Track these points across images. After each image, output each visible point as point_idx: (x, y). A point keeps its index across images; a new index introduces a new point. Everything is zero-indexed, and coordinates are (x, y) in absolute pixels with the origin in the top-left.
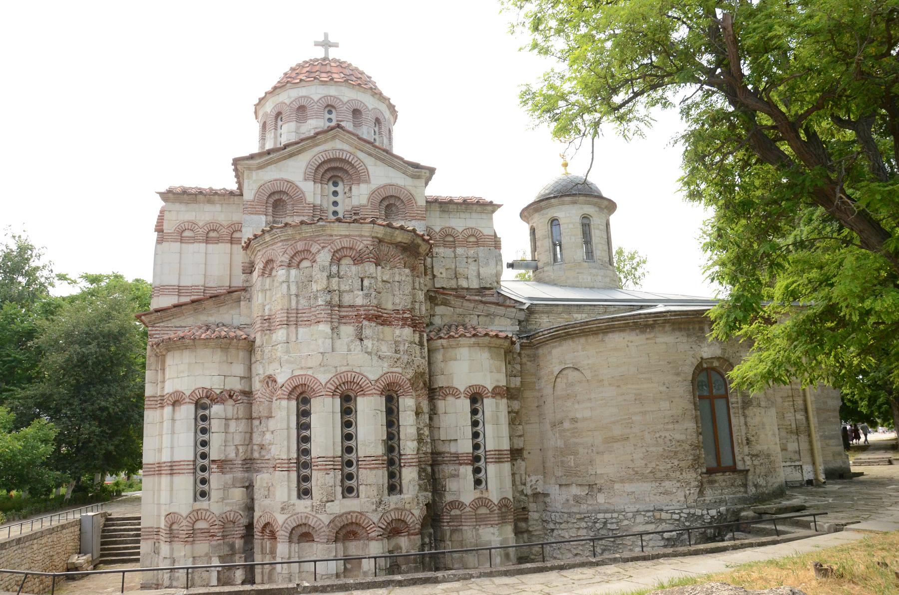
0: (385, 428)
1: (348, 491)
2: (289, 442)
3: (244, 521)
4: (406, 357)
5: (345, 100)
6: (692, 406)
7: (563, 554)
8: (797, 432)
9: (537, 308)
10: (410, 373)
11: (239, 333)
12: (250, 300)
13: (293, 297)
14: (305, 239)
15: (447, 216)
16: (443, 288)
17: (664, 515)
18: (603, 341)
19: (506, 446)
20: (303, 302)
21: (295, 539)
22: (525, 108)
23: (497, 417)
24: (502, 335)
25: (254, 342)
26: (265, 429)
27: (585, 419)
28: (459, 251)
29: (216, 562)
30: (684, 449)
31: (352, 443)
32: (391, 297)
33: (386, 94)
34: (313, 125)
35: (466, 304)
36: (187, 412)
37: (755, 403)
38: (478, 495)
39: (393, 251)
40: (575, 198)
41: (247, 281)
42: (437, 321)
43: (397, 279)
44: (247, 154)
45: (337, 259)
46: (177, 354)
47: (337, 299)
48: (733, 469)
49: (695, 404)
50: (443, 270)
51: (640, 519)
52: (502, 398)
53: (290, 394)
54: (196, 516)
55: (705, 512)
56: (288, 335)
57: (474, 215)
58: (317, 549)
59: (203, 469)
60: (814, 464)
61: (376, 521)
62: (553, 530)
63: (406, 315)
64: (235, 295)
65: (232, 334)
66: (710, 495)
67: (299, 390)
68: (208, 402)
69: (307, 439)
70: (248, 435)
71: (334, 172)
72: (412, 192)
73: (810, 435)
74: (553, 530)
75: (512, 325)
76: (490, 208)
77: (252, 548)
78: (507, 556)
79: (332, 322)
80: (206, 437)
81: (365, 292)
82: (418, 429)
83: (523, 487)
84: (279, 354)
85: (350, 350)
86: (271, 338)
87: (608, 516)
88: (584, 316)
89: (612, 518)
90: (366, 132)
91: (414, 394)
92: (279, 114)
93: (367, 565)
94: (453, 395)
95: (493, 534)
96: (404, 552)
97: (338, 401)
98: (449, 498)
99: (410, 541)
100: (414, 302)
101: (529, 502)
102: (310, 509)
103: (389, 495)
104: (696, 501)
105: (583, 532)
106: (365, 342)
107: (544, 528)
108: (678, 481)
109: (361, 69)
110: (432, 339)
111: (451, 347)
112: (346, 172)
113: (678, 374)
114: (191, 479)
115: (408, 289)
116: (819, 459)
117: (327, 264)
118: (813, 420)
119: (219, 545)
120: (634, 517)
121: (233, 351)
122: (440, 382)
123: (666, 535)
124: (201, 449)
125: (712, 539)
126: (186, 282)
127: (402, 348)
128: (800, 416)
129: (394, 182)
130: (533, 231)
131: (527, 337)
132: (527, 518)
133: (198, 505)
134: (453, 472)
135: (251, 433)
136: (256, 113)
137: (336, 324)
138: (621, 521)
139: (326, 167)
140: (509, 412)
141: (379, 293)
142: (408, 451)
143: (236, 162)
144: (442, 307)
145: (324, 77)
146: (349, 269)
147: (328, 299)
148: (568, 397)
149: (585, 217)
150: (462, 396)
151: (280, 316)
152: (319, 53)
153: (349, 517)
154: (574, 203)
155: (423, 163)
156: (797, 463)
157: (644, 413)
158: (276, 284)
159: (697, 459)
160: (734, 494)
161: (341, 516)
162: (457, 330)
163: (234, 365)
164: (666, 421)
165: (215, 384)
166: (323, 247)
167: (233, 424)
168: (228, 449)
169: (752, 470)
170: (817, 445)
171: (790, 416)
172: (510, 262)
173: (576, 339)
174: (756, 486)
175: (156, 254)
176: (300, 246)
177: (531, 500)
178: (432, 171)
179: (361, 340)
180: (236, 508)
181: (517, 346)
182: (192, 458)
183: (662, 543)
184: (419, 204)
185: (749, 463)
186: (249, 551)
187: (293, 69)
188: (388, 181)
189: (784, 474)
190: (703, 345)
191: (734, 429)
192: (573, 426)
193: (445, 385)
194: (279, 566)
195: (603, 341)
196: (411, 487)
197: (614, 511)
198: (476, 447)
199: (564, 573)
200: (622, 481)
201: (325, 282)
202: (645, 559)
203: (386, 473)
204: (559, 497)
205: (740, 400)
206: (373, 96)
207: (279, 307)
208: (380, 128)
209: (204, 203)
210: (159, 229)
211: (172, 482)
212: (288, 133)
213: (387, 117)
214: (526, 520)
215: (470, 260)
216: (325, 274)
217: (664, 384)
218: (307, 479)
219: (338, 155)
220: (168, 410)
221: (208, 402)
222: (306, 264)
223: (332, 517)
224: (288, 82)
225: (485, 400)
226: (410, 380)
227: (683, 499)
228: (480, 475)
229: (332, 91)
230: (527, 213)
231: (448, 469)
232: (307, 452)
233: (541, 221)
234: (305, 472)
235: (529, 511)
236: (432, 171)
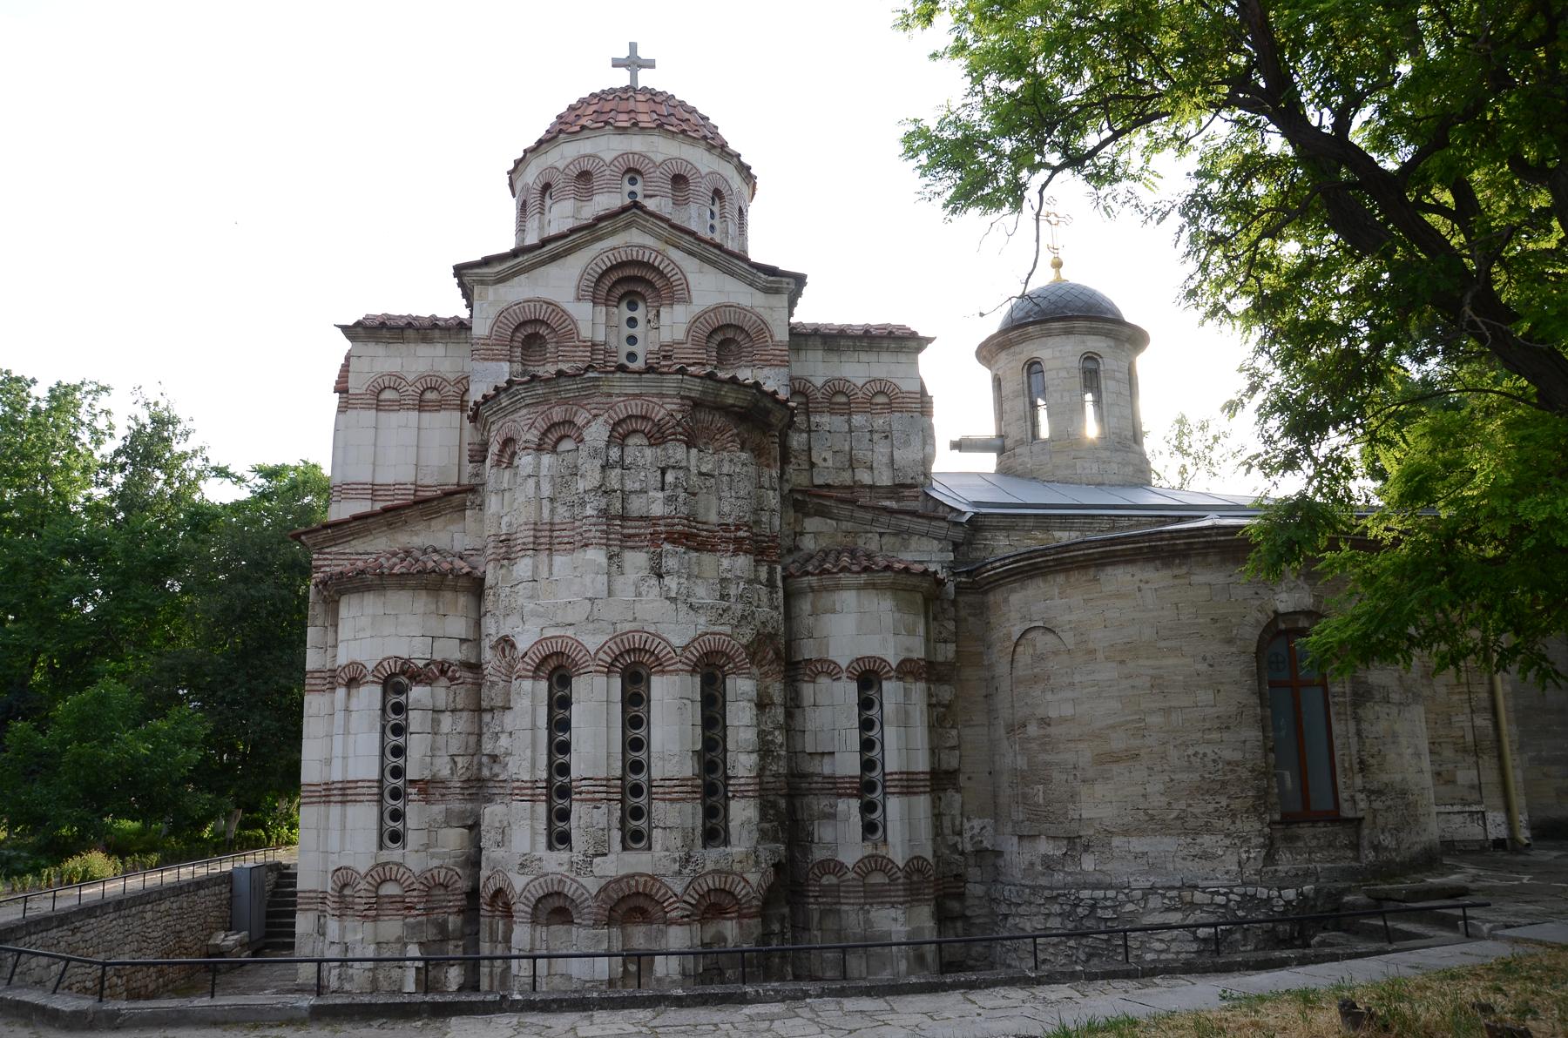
0: (699, 730)
1: (634, 839)
2: (534, 750)
3: (463, 884)
4: (740, 606)
5: (659, 159)
6: (1255, 700)
7: (1021, 959)
8: (1477, 750)
9: (987, 521)
10: (747, 635)
11: (458, 563)
12: (481, 507)
13: (546, 504)
14: (565, 401)
15: (836, 359)
16: (828, 486)
17: (1199, 897)
18: (1095, 580)
19: (922, 764)
20: (562, 510)
21: (543, 919)
22: (913, 163)
23: (907, 713)
24: (918, 568)
25: (481, 581)
26: (498, 729)
27: (1063, 720)
28: (858, 420)
29: (413, 951)
30: (1239, 779)
31: (641, 755)
32: (714, 500)
33: (733, 146)
34: (605, 202)
35: (859, 514)
36: (369, 697)
37: (1378, 697)
38: (869, 850)
39: (720, 421)
40: (1070, 324)
41: (477, 475)
42: (808, 544)
43: (725, 470)
44: (479, 258)
45: (620, 434)
47: (618, 505)
48: (1334, 818)
49: (1261, 696)
50: (828, 455)
51: (1155, 902)
52: (917, 678)
53: (538, 668)
54: (382, 873)
55: (1275, 893)
56: (536, 568)
57: (885, 357)
58: (580, 936)
59: (396, 794)
60: (1508, 810)
61: (679, 890)
62: (1006, 916)
63: (741, 534)
64: (454, 500)
65: (446, 566)
66: (1286, 863)
67: (553, 663)
68: (404, 680)
69: (565, 748)
70: (473, 739)
71: (630, 284)
72: (766, 317)
73: (1501, 757)
74: (1006, 916)
75: (941, 550)
76: (913, 344)
77: (477, 933)
78: (920, 960)
79: (608, 546)
80: (400, 740)
81: (668, 493)
82: (761, 734)
83: (957, 838)
84: (521, 601)
85: (640, 594)
86: (510, 571)
87: (1099, 894)
88: (1074, 534)
89: (1105, 899)
90: (695, 217)
91: (755, 670)
92: (547, 187)
93: (665, 968)
94: (829, 674)
95: (896, 920)
96: (730, 945)
97: (617, 682)
98: (819, 854)
99: (741, 927)
100: (758, 510)
101: (967, 866)
102: (566, 867)
103: (705, 847)
104: (1258, 872)
105: (1055, 923)
106: (667, 580)
107: (993, 913)
108: (1227, 836)
109: (690, 103)
110: (791, 575)
111: (826, 589)
112: (650, 284)
113: (1230, 641)
114: (373, 811)
115: (744, 488)
116: (1519, 801)
117: (602, 444)
118: (1508, 730)
119: (420, 924)
120: (1145, 897)
121: (448, 595)
122: (808, 650)
123: (1202, 932)
124: (391, 761)
125: (1287, 943)
126: (386, 477)
127: (733, 591)
128: (1483, 721)
129: (733, 300)
130: (998, 382)
131: (969, 573)
132: (963, 894)
133: (385, 856)
134: (827, 810)
135: (480, 735)
136: (511, 185)
137: (616, 549)
138: (1122, 904)
139: (614, 277)
140: (929, 705)
141: (694, 494)
142: (741, 772)
143: (459, 271)
144: (817, 520)
145: (623, 120)
146: (641, 453)
147: (603, 506)
148: (1035, 679)
149: (1090, 357)
150: (844, 676)
151: (525, 536)
152: (621, 78)
153: (633, 883)
154: (1068, 332)
155: (783, 267)
156: (1474, 808)
157: (1167, 711)
158: (519, 480)
159: (1262, 795)
160: (1333, 861)
161: (618, 881)
162: (838, 559)
163: (449, 619)
164: (1207, 725)
165: (417, 651)
166: (596, 416)
167: (446, 722)
168: (437, 761)
169: (1369, 818)
170: (1515, 776)
171: (1462, 720)
172: (957, 439)
173: (1049, 578)
174: (1376, 848)
175: (336, 430)
176: (558, 414)
177: (972, 861)
178: (800, 280)
179: (660, 576)
180: (449, 862)
181: (950, 587)
182: (376, 776)
183: (1195, 947)
184: (777, 338)
185: (1362, 805)
186: (471, 936)
187: (571, 108)
188: (723, 300)
189: (1438, 824)
190: (1278, 589)
191: (1337, 743)
192: (1042, 732)
193: (814, 656)
194: (514, 963)
195: (1095, 580)
196: (745, 833)
197: (1110, 887)
198: (867, 765)
199: (976, 996)
200: (1126, 833)
201: (597, 475)
202: (1128, 975)
203: (700, 809)
204: (1019, 857)
205: (1347, 690)
206: (709, 150)
207: (522, 520)
208: (722, 207)
209: (416, 341)
210: (341, 388)
211: (344, 816)
212: (561, 216)
213: (735, 187)
214: (961, 896)
215: (876, 437)
216: (598, 463)
217: (1204, 659)
218: (565, 815)
219: (635, 255)
220: (341, 692)
221: (404, 680)
222: (567, 445)
223: (603, 882)
224: (561, 131)
225: (885, 684)
226: (746, 647)
227: (1235, 868)
228: (874, 816)
229: (636, 144)
230: (989, 351)
231: (822, 804)
232: (564, 769)
233: (1012, 363)
234: (560, 803)
235: (966, 882)
236: (800, 280)
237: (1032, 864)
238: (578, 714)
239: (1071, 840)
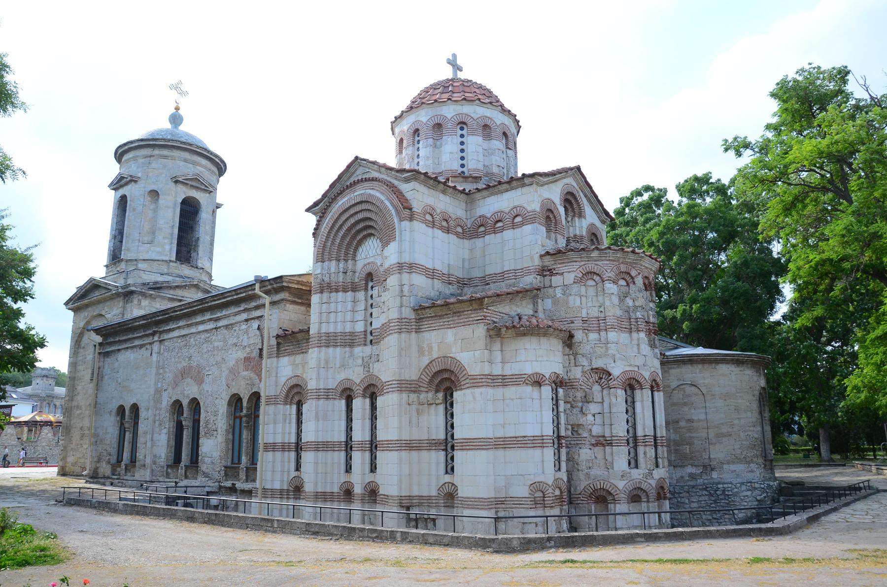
17: (757, 485)
25: (571, 336)
27: (699, 421)
36: (547, 391)
46: (534, 339)
51: (744, 488)
87: (725, 486)
148: (685, 404)
157: (739, 419)
176: (623, 268)
183: (756, 503)
200: (728, 463)
237: (682, 477)
238: (638, 405)
239: (705, 467)
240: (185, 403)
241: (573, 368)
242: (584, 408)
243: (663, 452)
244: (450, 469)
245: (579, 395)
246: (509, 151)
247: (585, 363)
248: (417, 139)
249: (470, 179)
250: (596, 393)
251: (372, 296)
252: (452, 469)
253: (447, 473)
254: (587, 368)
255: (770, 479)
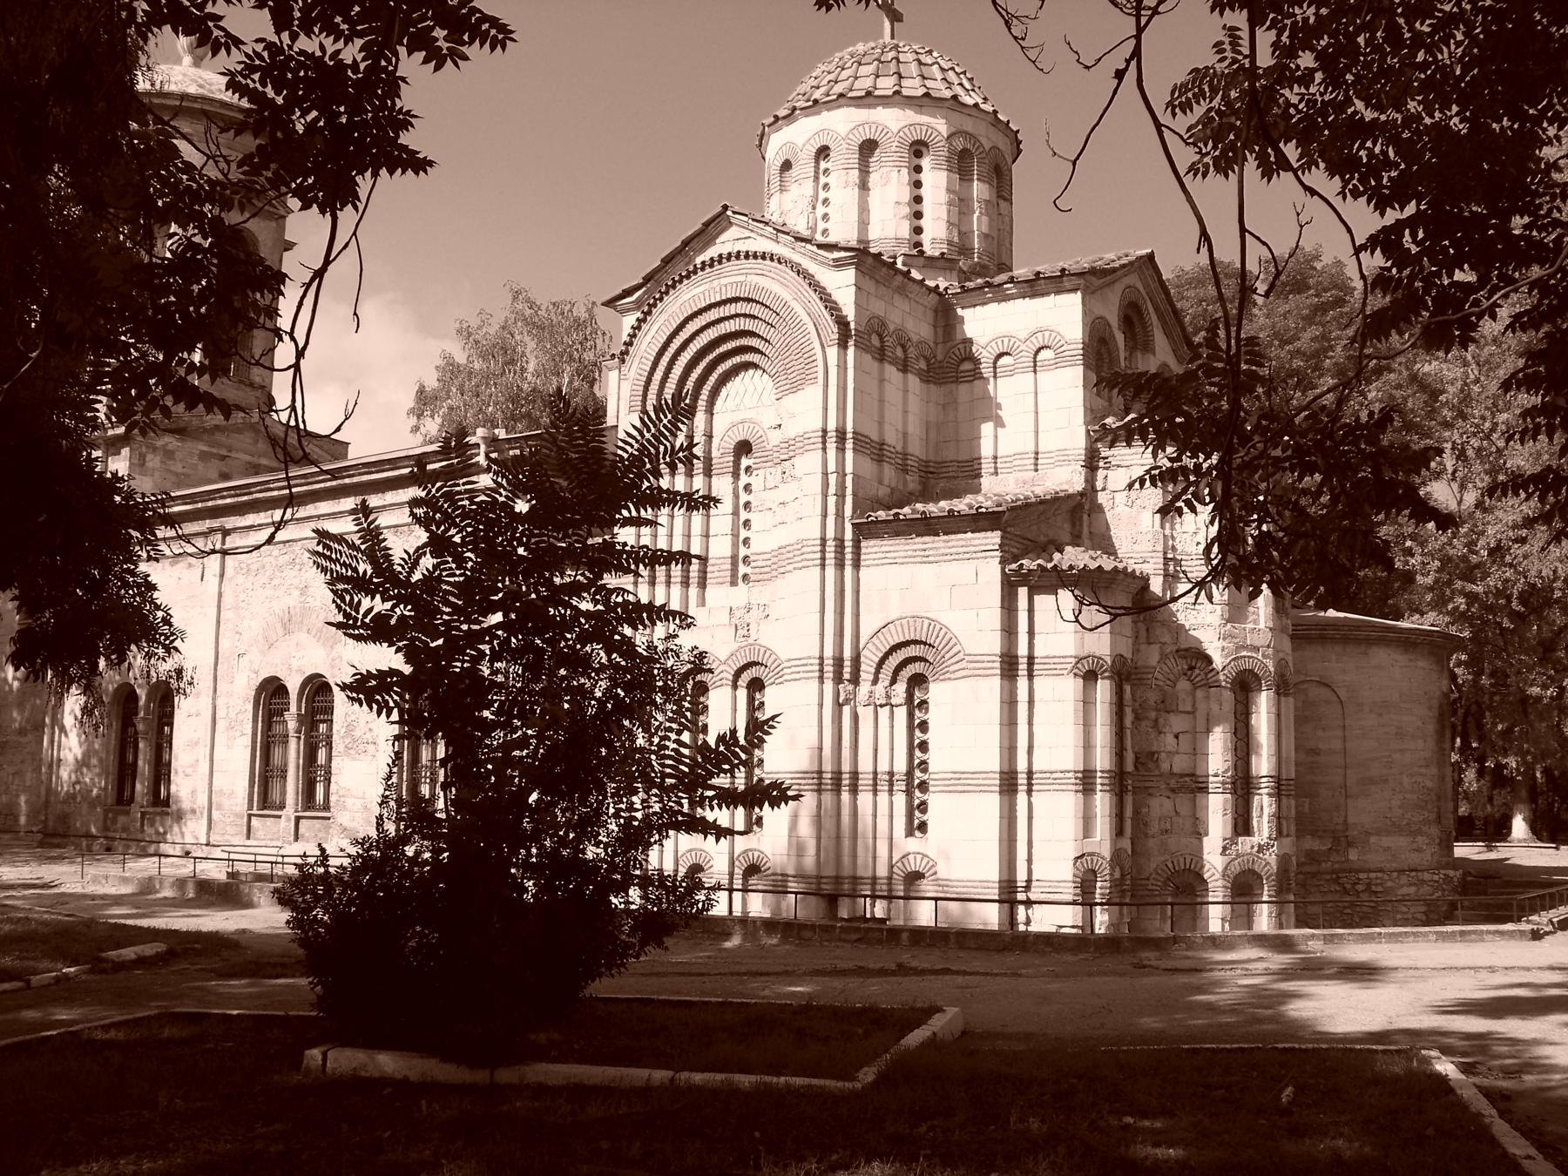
17: (1426, 876)
51: (1404, 880)
87: (1373, 875)
113: (1430, 708)
197: (1370, 871)
200: (1378, 833)
239: (1336, 840)
240: (293, 685)
241: (1143, 647)
242: (1161, 721)
243: (1289, 807)
244: (917, 827)
245: (1152, 697)
246: (1002, 202)
247: (1167, 638)
248: (823, 165)
249: (941, 263)
250: (1182, 696)
251: (747, 488)
252: (923, 827)
253: (910, 833)
254: (1170, 649)
255: (1447, 866)
